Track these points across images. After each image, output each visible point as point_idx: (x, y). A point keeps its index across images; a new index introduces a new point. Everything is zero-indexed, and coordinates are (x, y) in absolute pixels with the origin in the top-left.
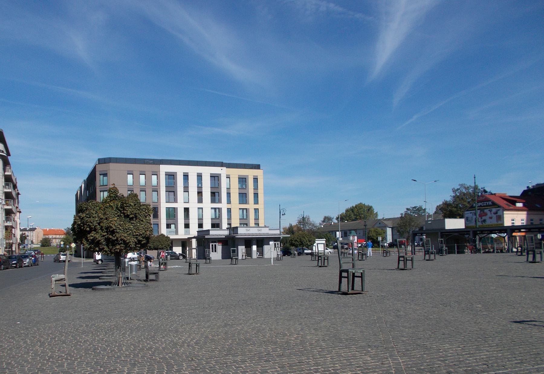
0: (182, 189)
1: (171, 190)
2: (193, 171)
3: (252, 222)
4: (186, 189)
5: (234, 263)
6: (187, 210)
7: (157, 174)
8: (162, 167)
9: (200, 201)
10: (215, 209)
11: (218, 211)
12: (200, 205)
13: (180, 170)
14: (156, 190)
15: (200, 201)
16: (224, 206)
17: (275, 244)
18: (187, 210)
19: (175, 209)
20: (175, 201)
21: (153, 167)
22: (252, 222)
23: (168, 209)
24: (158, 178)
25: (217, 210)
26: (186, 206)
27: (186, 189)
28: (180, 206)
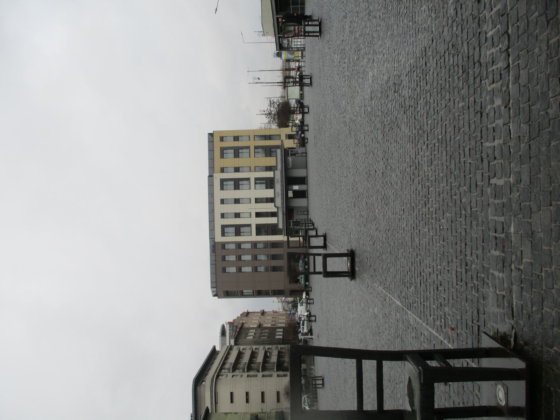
0: (237, 219)
1: (238, 229)
2: (219, 209)
4: (237, 215)
6: (258, 215)
7: (223, 245)
10: (255, 183)
11: (258, 180)
12: (253, 201)
16: (253, 176)
17: (292, 155)
18: (258, 215)
20: (249, 225)
21: (219, 247)
23: (258, 233)
24: (228, 243)
25: (257, 182)
26: (254, 215)
27: (237, 215)
28: (255, 221)
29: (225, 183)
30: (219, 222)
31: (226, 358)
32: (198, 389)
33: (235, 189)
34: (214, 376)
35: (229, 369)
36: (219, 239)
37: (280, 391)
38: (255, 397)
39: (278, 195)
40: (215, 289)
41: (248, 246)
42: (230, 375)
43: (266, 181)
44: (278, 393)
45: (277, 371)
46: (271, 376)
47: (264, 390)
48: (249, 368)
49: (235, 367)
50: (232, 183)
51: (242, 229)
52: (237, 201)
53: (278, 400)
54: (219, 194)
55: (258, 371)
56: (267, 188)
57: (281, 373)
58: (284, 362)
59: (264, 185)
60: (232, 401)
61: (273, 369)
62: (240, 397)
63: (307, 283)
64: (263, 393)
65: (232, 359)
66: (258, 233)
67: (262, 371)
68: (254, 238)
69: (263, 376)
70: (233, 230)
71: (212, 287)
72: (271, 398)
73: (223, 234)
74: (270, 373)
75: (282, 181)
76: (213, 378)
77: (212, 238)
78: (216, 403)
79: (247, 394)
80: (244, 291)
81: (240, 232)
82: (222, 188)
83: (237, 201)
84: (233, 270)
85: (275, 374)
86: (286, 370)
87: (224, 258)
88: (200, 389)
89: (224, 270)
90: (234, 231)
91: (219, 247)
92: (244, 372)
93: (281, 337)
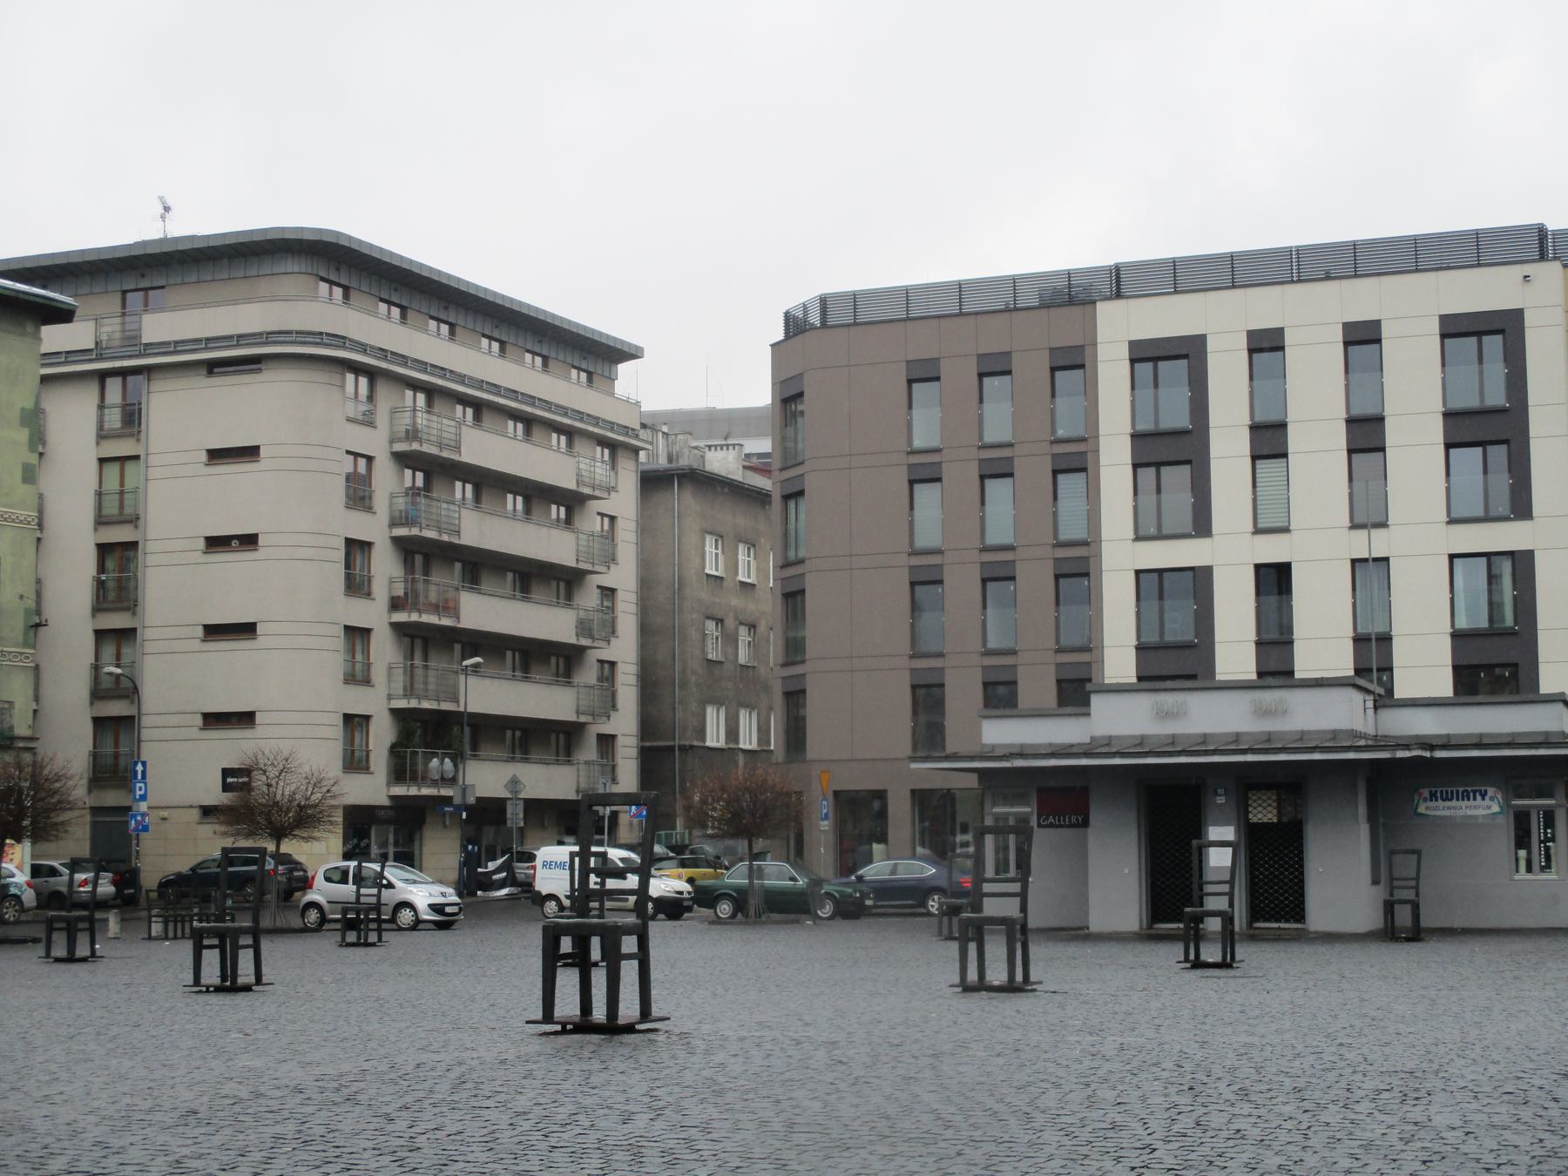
1: (1172, 451)
3: (1235, 653)
4: (1269, 440)
5: (997, 975)
6: (1274, 581)
7: (1073, 361)
8: (1104, 310)
9: (1368, 514)
13: (1224, 322)
14: (1075, 461)
15: (1368, 514)
18: (1274, 581)
19: (1200, 580)
20: (1202, 526)
22: (1235, 653)
23: (1152, 583)
26: (1272, 550)
27: (1269, 440)
28: (1231, 556)
29: (1494, 344)
30: (1224, 322)
32: (292, 265)
33: (1448, 415)
34: (363, 348)
35: (413, 434)
36: (1118, 327)
37: (258, 731)
38: (231, 588)
39: (1164, 715)
40: (815, 318)
41: (1071, 529)
42: (376, 442)
43: (1510, 633)
44: (246, 719)
45: (396, 713)
46: (358, 677)
47: (262, 641)
49: (438, 471)
50: (1497, 397)
51: (1176, 478)
52: (1366, 435)
53: (214, 720)
54: (1410, 311)
55: (395, 604)
56: (1457, 636)
57: (382, 735)
58: (458, 758)
59: (1483, 623)
60: (217, 455)
61: (409, 691)
62: (234, 500)
63: (827, 910)
64: (246, 630)
65: (486, 447)
66: (1152, 583)
68: (1122, 558)
69: (357, 635)
70: (1176, 416)
71: (824, 302)
72: (226, 677)
73: (1146, 354)
74: (378, 673)
75: (1173, 745)
76: (341, 340)
77: (1117, 282)
78: (212, 367)
79: (249, 541)
80: (803, 504)
81: (1158, 465)
82: (1454, 328)
83: (1366, 435)
84: (926, 429)
85: (376, 702)
86: (401, 770)
87: (994, 367)
88: (292, 278)
89: (923, 374)
90: (1167, 424)
91: (1062, 329)
93: (715, 738)
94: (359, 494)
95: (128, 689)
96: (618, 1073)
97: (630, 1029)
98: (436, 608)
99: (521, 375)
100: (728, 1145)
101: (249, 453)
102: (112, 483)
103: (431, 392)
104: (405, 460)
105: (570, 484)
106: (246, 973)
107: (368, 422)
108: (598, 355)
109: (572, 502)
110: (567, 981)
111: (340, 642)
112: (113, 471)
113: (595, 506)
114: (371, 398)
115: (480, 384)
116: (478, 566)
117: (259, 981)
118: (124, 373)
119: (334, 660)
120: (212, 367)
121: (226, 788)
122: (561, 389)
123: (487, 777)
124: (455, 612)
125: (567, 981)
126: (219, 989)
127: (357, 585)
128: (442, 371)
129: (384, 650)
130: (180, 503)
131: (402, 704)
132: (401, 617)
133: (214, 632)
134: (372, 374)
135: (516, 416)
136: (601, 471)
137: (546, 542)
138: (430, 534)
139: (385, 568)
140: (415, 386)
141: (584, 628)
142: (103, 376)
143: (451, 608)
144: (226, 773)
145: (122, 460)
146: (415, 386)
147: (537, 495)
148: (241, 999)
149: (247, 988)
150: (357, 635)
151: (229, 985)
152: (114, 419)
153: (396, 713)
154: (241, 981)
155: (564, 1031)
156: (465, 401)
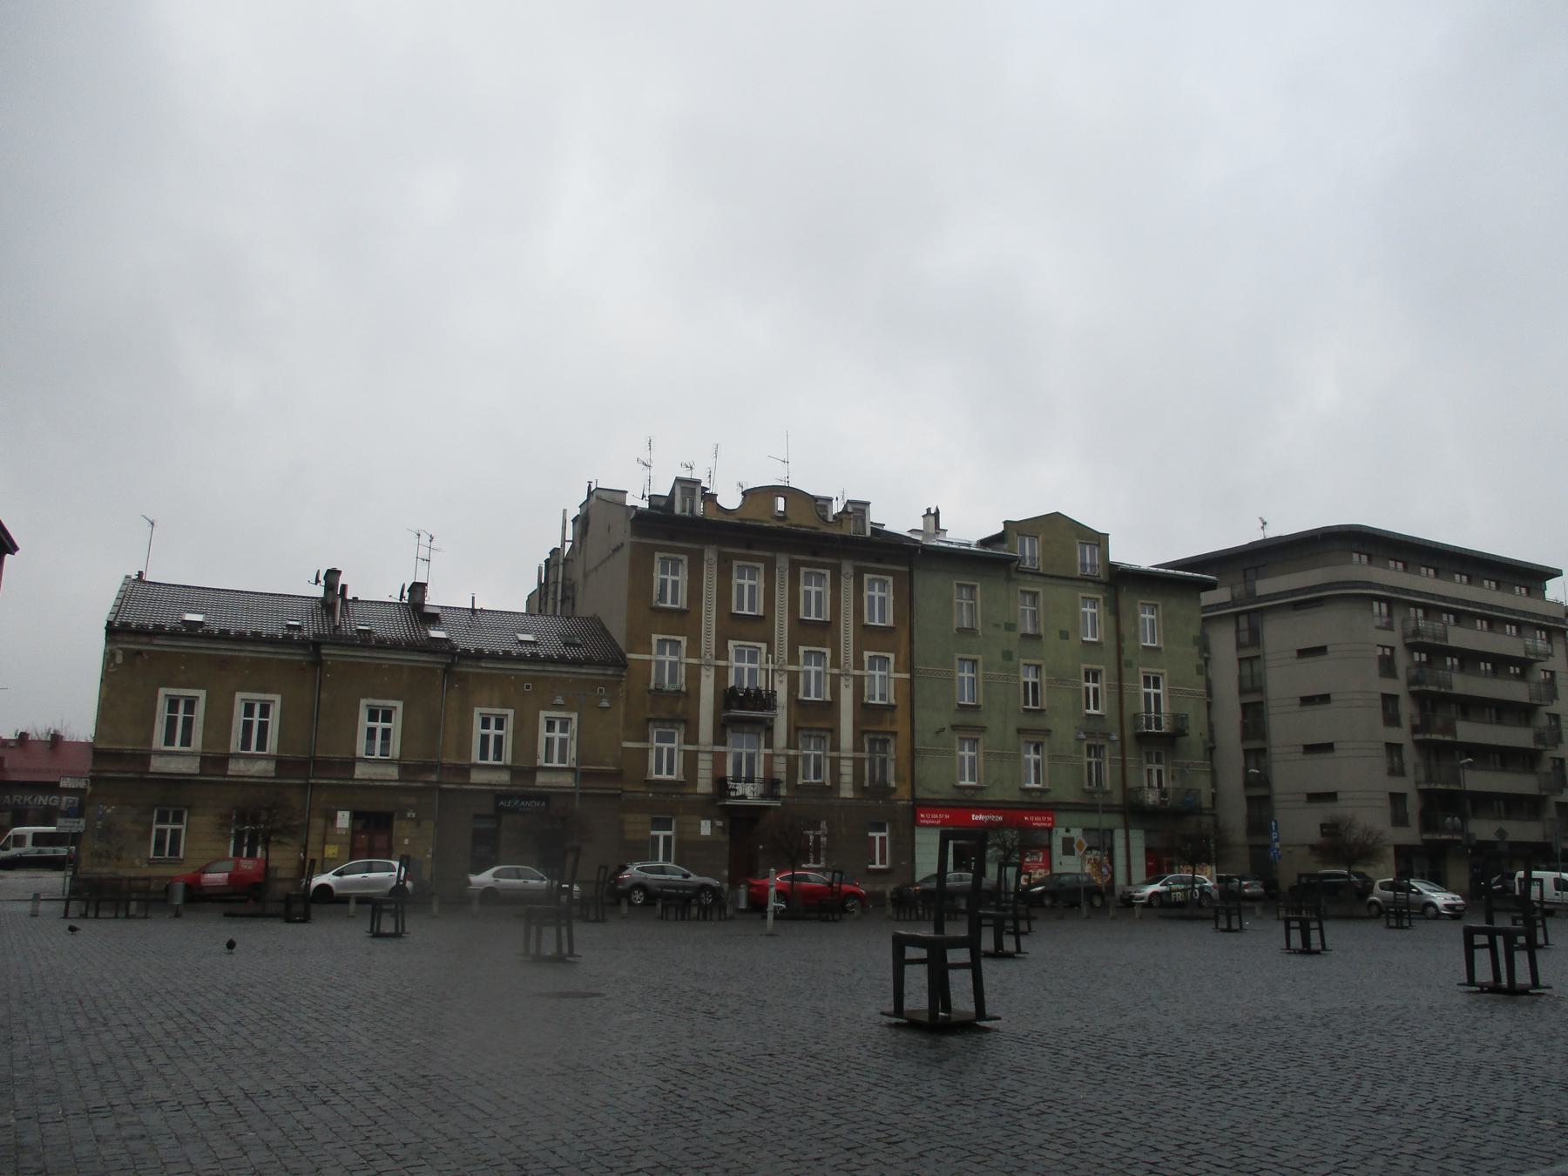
31: (1495, 620)
34: (1382, 587)
35: (1417, 632)
38: (1318, 725)
42: (1394, 638)
44: (1331, 797)
45: (1421, 791)
46: (1396, 771)
48: (1431, 702)
53: (1314, 797)
55: (1415, 729)
57: (1413, 806)
58: (1464, 818)
60: (1303, 653)
61: (1429, 779)
62: (1314, 677)
64: (1327, 747)
65: (1461, 637)
67: (1417, 743)
69: (1393, 749)
72: (1319, 773)
76: (1369, 585)
79: (1325, 699)
86: (1427, 824)
92: (1410, 683)
94: (1387, 666)
95: (1264, 780)
96: (1502, 1020)
97: (1524, 992)
98: (1443, 732)
99: (1487, 593)
100: (1538, 1072)
101: (1321, 650)
102: (1247, 671)
103: (1427, 609)
104: (1412, 648)
105: (1522, 654)
106: (1315, 942)
107: (1389, 627)
108: (1534, 577)
109: (1525, 665)
110: (1483, 958)
111: (1383, 752)
112: (1246, 665)
113: (1538, 665)
114: (1390, 614)
115: (1457, 601)
116: (1471, 706)
117: (1324, 948)
118: (1248, 612)
119: (1381, 763)
120: (1297, 606)
121: (1323, 834)
122: (1515, 599)
123: (1483, 829)
124: (1453, 732)
125: (1483, 958)
126: (1301, 952)
127: (1392, 719)
128: (1432, 596)
129: (1410, 756)
130: (1284, 680)
131: (1425, 786)
132: (1419, 737)
133: (1310, 749)
134: (1389, 601)
135: (1482, 617)
136: (1541, 645)
137: (1513, 690)
138: (1434, 688)
139: (1407, 710)
140: (1417, 605)
141: (1539, 738)
142: (1237, 615)
143: (1451, 730)
144: (1323, 826)
145: (1250, 659)
146: (1417, 605)
147: (1500, 663)
148: (1308, 959)
149: (1317, 952)
150: (1393, 749)
151: (1307, 950)
152: (1245, 637)
153: (1421, 791)
154: (1314, 947)
155: (1482, 991)
156: (1449, 611)
